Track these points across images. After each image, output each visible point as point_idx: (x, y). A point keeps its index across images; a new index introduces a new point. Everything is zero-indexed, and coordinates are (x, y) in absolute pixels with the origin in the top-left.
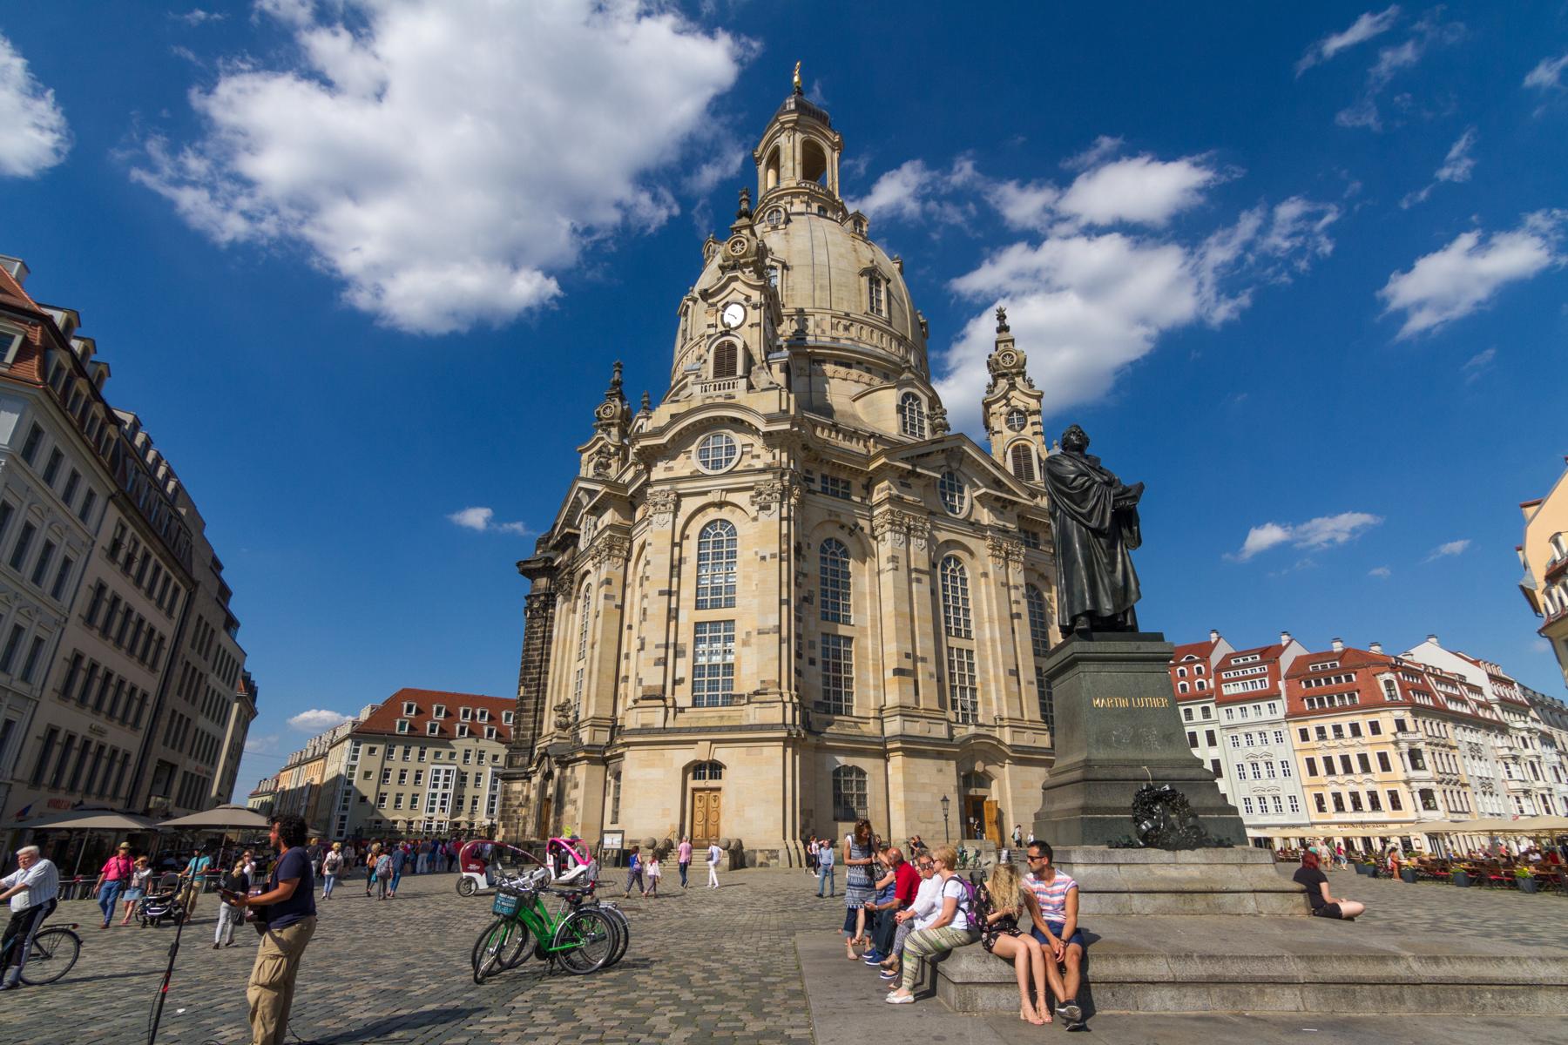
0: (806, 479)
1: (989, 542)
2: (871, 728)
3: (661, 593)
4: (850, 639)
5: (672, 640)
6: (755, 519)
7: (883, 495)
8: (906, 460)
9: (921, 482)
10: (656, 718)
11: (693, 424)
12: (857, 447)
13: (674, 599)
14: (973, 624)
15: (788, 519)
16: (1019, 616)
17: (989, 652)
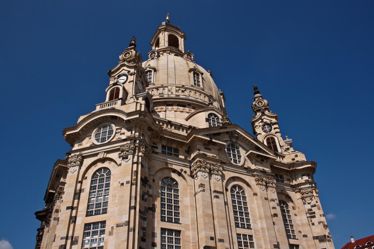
0: (152, 147)
3: (68, 208)
4: (178, 232)
5: (70, 234)
6: (120, 165)
8: (207, 136)
9: (217, 148)
13: (74, 211)
14: (251, 221)
15: (137, 163)
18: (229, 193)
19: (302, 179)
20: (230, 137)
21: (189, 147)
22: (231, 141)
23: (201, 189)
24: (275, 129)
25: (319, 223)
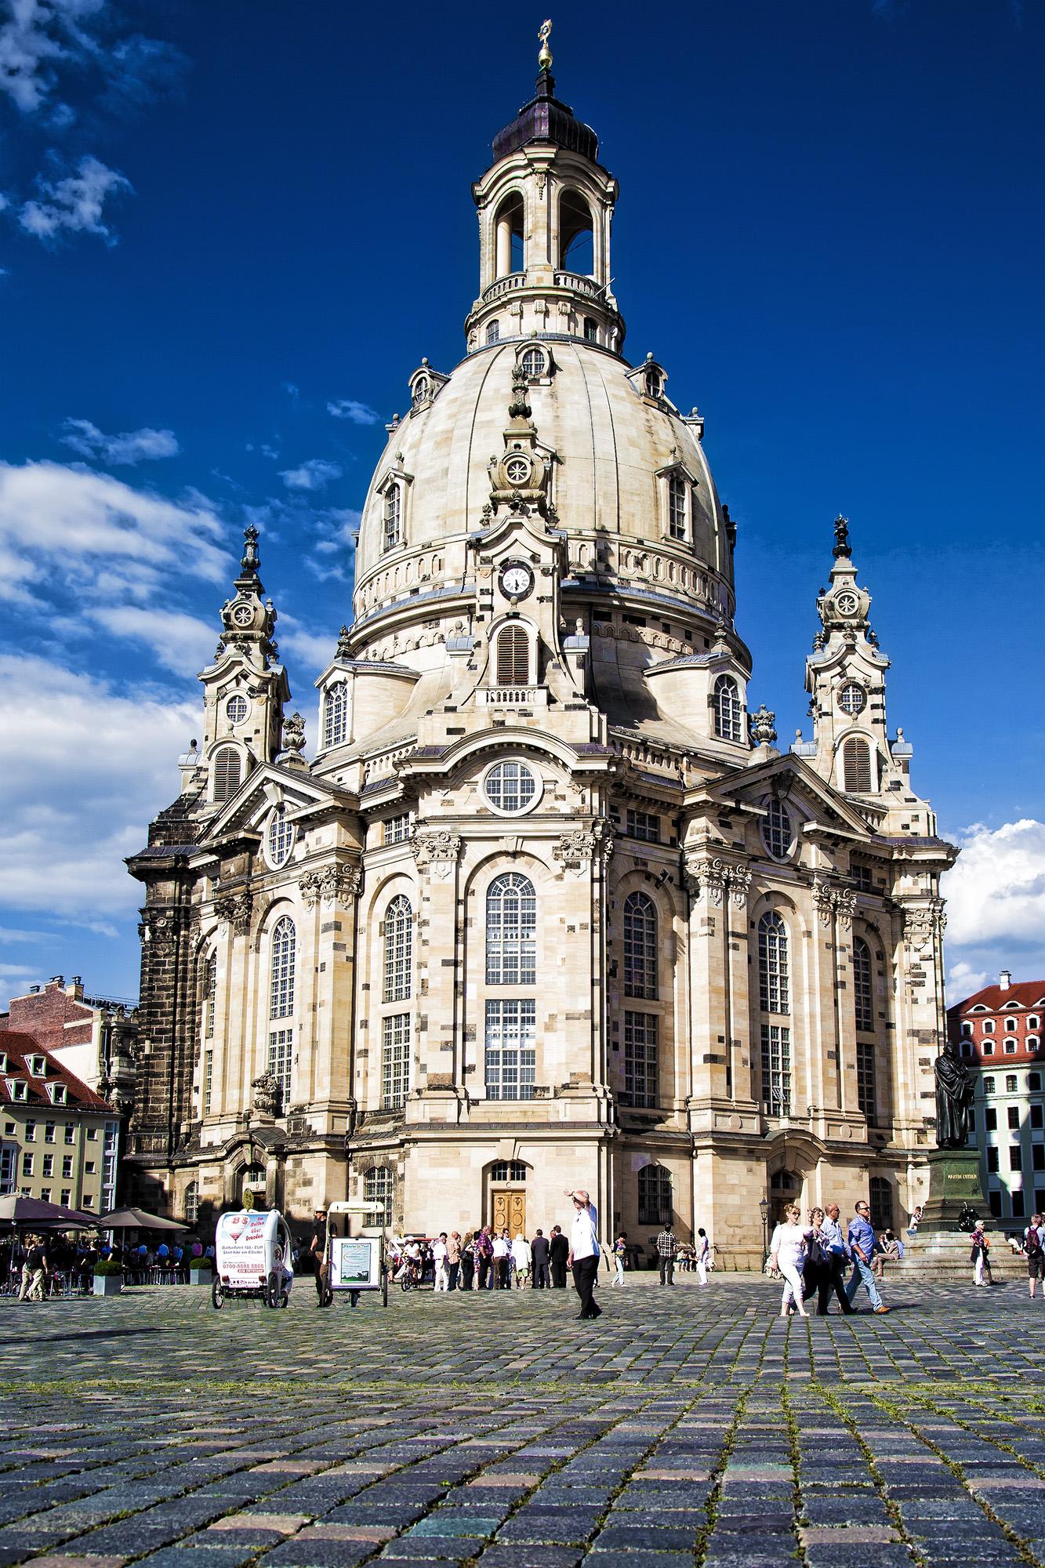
1: (815, 892)
2: (676, 1122)
3: (445, 963)
5: (460, 1021)
6: (560, 877)
7: (700, 838)
8: (729, 795)
9: (743, 820)
10: (448, 1111)
11: (483, 749)
12: (667, 770)
13: (460, 970)
14: (790, 996)
15: (601, 880)
16: (843, 984)
17: (807, 1029)
18: (756, 932)
19: (915, 883)
20: (773, 784)
21: (683, 814)
22: (775, 794)
23: (706, 930)
24: (874, 707)
25: (929, 1000)
